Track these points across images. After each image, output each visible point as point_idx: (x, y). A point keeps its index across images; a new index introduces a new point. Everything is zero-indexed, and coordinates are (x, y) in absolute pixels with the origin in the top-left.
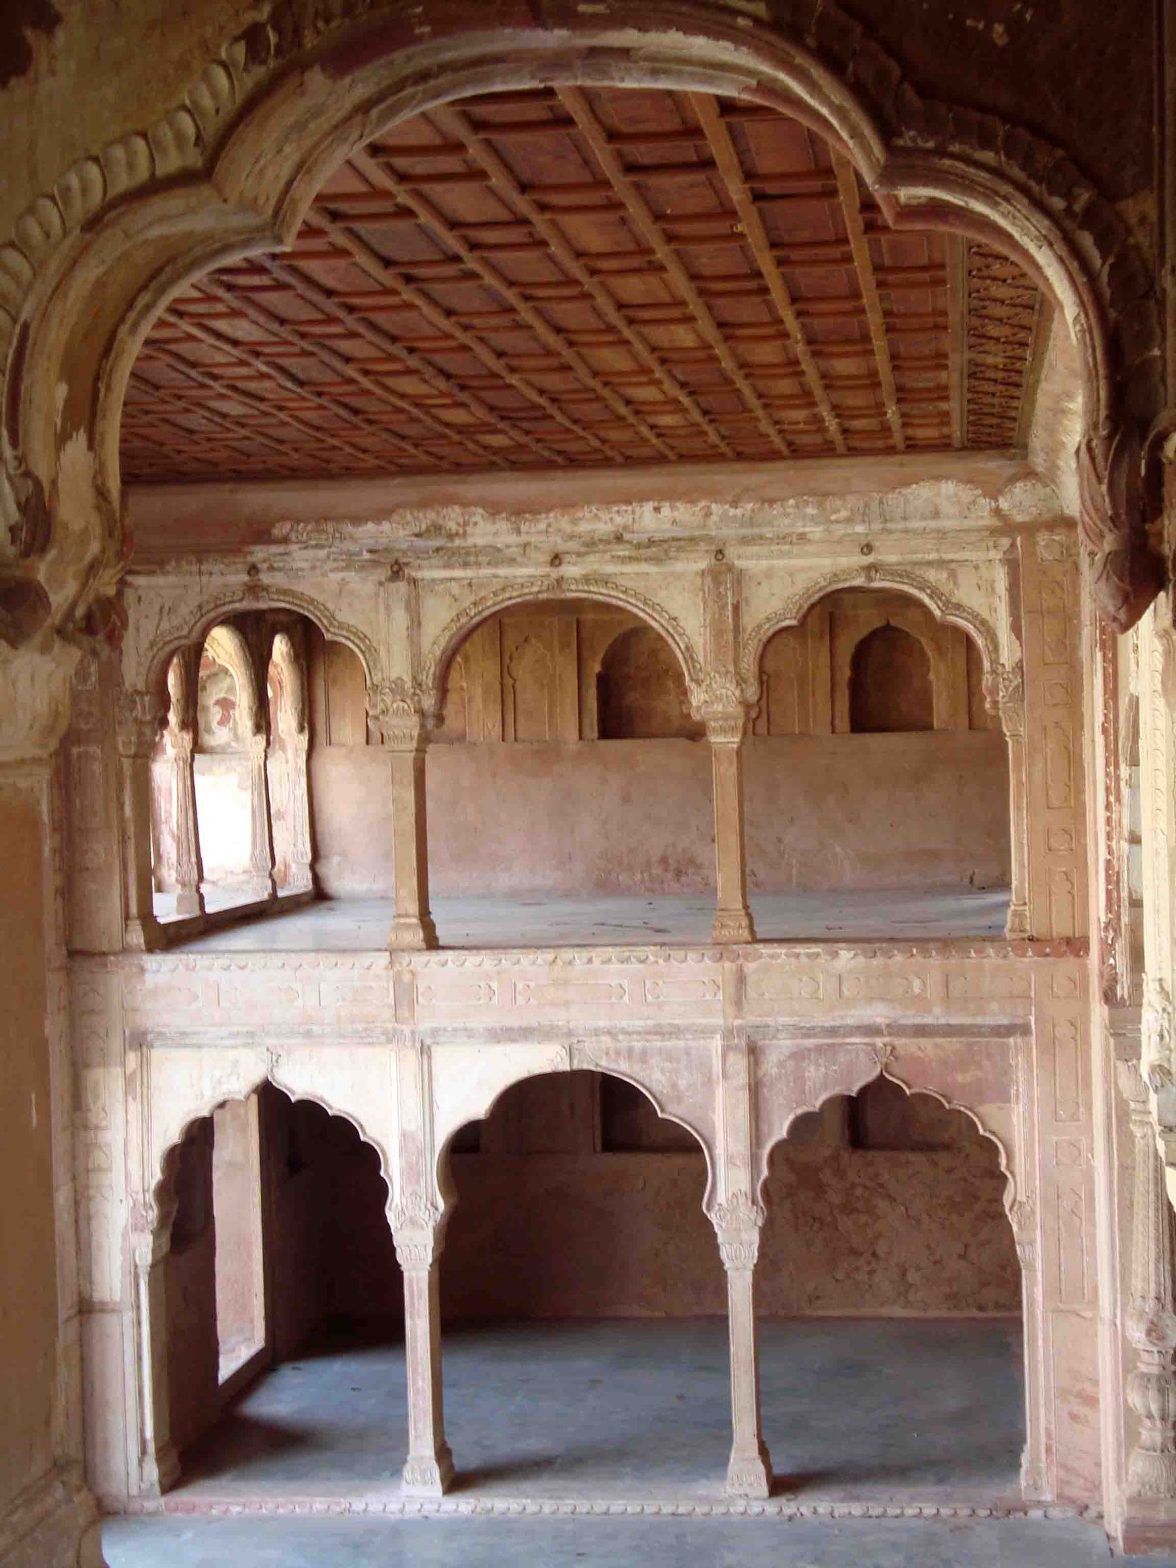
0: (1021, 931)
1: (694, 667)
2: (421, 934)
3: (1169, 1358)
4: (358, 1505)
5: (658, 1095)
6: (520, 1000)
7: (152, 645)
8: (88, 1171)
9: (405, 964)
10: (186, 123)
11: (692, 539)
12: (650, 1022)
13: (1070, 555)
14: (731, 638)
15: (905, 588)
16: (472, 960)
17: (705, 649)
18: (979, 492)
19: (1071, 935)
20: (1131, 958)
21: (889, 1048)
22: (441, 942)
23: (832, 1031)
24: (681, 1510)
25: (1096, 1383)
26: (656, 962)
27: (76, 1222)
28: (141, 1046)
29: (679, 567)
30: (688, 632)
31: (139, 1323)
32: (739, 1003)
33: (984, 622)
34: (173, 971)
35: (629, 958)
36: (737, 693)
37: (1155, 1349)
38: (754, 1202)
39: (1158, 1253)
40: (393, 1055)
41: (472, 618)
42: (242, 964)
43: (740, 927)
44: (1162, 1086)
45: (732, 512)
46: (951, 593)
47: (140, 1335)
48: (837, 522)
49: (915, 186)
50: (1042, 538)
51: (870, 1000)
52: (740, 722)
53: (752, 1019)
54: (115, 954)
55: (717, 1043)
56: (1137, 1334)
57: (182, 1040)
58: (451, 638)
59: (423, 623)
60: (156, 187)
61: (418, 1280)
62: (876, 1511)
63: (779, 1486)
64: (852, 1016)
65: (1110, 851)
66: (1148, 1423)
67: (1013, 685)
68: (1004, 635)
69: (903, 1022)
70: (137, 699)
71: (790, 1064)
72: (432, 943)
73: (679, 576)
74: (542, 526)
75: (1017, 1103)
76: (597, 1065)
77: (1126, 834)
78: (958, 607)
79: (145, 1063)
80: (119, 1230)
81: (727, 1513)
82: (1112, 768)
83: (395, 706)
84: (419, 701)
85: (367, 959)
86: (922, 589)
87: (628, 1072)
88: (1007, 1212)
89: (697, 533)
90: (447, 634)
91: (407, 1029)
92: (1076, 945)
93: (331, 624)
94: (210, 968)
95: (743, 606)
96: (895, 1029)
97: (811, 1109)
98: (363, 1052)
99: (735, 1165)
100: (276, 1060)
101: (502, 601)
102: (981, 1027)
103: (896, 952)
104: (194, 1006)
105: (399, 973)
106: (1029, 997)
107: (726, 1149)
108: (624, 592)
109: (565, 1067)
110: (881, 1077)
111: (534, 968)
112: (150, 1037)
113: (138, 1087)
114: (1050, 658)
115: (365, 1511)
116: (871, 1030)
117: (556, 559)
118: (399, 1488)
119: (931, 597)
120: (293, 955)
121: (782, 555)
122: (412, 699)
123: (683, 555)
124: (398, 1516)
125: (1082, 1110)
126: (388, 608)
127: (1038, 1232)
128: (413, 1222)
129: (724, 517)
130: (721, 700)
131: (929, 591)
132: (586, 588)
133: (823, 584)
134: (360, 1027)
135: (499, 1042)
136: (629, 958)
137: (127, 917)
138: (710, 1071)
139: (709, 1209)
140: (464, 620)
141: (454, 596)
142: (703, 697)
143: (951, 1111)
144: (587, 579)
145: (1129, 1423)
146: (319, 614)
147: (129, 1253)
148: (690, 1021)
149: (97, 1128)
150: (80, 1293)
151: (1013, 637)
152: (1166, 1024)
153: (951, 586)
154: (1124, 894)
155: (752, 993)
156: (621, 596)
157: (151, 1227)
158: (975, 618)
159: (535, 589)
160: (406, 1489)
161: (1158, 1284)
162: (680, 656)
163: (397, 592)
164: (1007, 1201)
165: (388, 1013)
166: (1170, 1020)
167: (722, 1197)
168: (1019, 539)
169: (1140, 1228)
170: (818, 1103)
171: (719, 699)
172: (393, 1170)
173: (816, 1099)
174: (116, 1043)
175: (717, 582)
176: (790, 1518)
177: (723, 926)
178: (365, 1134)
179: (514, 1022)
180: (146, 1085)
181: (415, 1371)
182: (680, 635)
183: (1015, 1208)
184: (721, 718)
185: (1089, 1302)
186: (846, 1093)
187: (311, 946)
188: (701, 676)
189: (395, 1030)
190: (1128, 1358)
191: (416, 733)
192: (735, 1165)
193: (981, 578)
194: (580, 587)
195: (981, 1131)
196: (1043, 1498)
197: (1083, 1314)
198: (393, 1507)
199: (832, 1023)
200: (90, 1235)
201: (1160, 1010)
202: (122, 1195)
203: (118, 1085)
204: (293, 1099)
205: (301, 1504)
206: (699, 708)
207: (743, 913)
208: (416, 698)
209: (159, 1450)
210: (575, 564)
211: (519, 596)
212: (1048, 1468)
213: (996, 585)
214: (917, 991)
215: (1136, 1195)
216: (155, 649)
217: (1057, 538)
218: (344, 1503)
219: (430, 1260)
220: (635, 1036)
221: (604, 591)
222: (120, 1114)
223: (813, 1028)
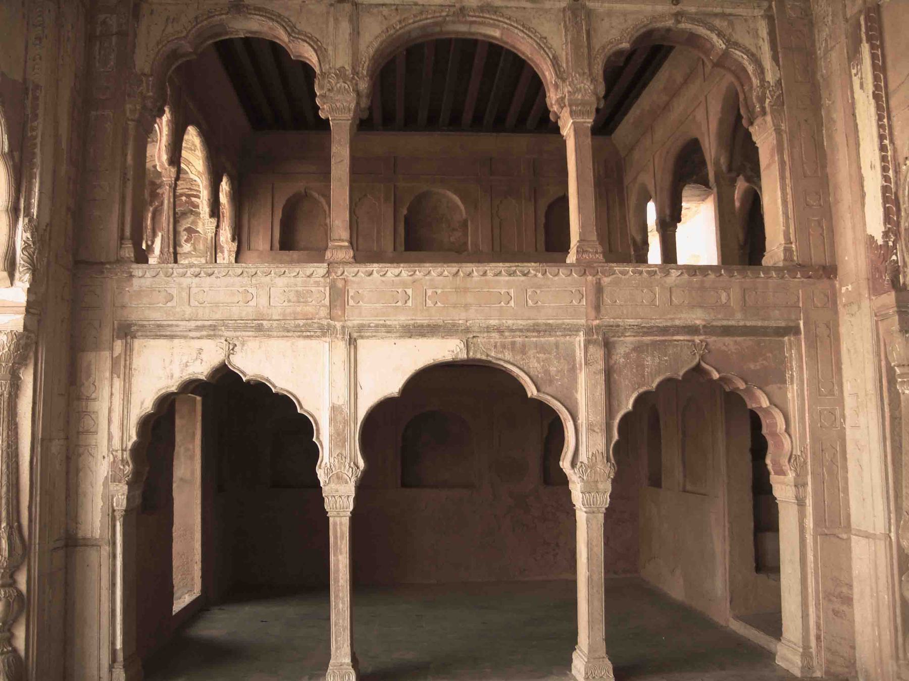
0: (791, 261)
1: (560, 71)
2: (351, 253)
5: (535, 378)
6: (429, 303)
7: (158, 44)
8: (78, 433)
9: (339, 273)
12: (531, 322)
13: (807, 15)
14: (586, 50)
17: (567, 58)
19: (824, 264)
21: (704, 344)
23: (664, 331)
25: (850, 586)
26: (536, 275)
27: (67, 473)
28: (126, 335)
30: (555, 46)
31: (114, 556)
32: (597, 308)
33: (753, 55)
35: (515, 272)
36: (592, 87)
38: (608, 460)
40: (327, 345)
41: (397, 31)
42: (210, 271)
43: (596, 252)
46: (730, 34)
47: (114, 565)
49: (455, 194)
51: (692, 307)
53: (608, 320)
54: (109, 263)
55: (581, 338)
57: (160, 332)
58: (382, 43)
59: (361, 32)
61: (341, 523)
64: (680, 319)
67: (777, 93)
68: (768, 63)
69: (715, 323)
70: (144, 79)
71: (634, 355)
73: (546, 11)
75: (792, 383)
76: (488, 355)
79: (128, 350)
82: (885, 120)
83: (338, 85)
84: (357, 84)
90: (379, 40)
91: (338, 325)
93: (293, 30)
94: (184, 275)
95: (592, 33)
96: (709, 330)
97: (650, 388)
98: (302, 343)
99: (594, 431)
100: (232, 350)
101: (421, 20)
102: (767, 327)
103: (710, 272)
104: (169, 304)
105: (334, 281)
106: (799, 307)
107: (587, 418)
108: (509, 19)
109: (463, 356)
110: (699, 365)
111: (441, 278)
112: (134, 328)
113: (122, 367)
114: (800, 78)
116: (692, 330)
119: (719, 35)
122: (351, 82)
125: (836, 387)
126: (336, 20)
127: (809, 477)
128: (339, 478)
130: (580, 91)
131: (717, 32)
132: (481, 15)
134: (301, 322)
136: (515, 272)
137: (122, 238)
138: (574, 360)
140: (392, 31)
141: (384, 16)
146: (284, 24)
147: (108, 498)
148: (560, 322)
150: (67, 531)
151: (774, 64)
153: (731, 31)
155: (607, 300)
156: (508, 21)
158: (747, 51)
159: (444, 14)
163: (344, 10)
165: (324, 312)
170: (654, 385)
171: (579, 90)
172: (324, 436)
173: (653, 382)
174: (107, 333)
175: (575, 14)
178: (301, 407)
179: (422, 320)
180: (129, 368)
181: (337, 596)
182: (549, 49)
183: (792, 461)
184: (580, 104)
185: (845, 527)
186: (675, 376)
188: (565, 76)
189: (329, 324)
191: (353, 106)
192: (594, 431)
193: (749, 27)
194: (477, 14)
196: (814, 675)
197: (840, 536)
199: (665, 324)
200: (77, 486)
202: (105, 452)
204: (244, 379)
208: (354, 82)
209: (125, 659)
211: (433, 17)
212: (818, 652)
213: (760, 32)
214: (724, 300)
216: (160, 47)
217: (798, 4)
219: (351, 508)
220: (518, 333)
221: (495, 17)
223: (652, 327)
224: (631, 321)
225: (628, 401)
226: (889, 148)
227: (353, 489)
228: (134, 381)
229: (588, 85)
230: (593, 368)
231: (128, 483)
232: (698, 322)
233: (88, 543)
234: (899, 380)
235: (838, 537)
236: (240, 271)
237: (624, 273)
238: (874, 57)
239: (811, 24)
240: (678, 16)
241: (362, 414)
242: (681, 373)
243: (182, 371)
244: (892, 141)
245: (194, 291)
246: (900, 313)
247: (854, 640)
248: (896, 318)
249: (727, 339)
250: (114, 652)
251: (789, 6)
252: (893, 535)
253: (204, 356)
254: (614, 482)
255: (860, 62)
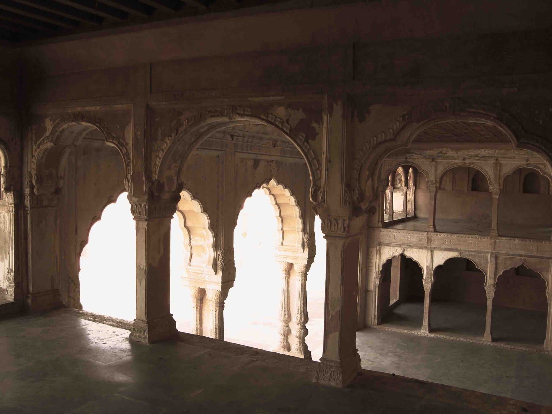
2: (433, 229)
4: (413, 332)
8: (368, 267)
10: (391, 131)
11: (492, 157)
15: (535, 169)
16: (442, 235)
22: (437, 231)
23: (513, 255)
24: (474, 342)
28: (380, 245)
29: (488, 162)
31: (376, 295)
32: (494, 248)
34: (386, 232)
36: (499, 187)
38: (494, 286)
41: (447, 169)
45: (500, 152)
48: (521, 155)
52: (499, 193)
54: (376, 228)
55: (489, 255)
57: (387, 245)
58: (444, 172)
60: (385, 141)
62: (513, 347)
63: (494, 340)
72: (435, 231)
74: (462, 153)
76: (465, 257)
78: (546, 173)
79: (380, 248)
80: (373, 278)
81: (483, 344)
83: (431, 185)
84: (436, 185)
85: (423, 233)
86: (539, 169)
87: (471, 259)
88: (546, 293)
89: (493, 155)
90: (442, 172)
94: (393, 232)
96: (526, 256)
100: (404, 251)
108: (478, 166)
109: (459, 257)
110: (522, 265)
115: (414, 333)
116: (521, 256)
117: (464, 159)
118: (420, 330)
119: (540, 171)
120: (409, 231)
121: (509, 161)
123: (490, 160)
124: (420, 335)
128: (427, 283)
129: (498, 153)
133: (518, 167)
134: (420, 245)
135: (446, 251)
137: (379, 221)
138: (488, 260)
139: (485, 286)
142: (492, 187)
143: (536, 273)
144: (470, 163)
149: (371, 259)
156: (477, 167)
157: (379, 278)
159: (460, 165)
160: (422, 331)
162: (488, 179)
164: (547, 291)
165: (426, 243)
167: (488, 284)
170: (509, 269)
174: (375, 244)
176: (496, 346)
177: (493, 233)
181: (425, 310)
182: (488, 175)
187: (413, 229)
189: (427, 247)
195: (542, 277)
198: (419, 333)
203: (375, 251)
204: (407, 257)
205: (402, 331)
206: (491, 190)
207: (496, 230)
210: (468, 160)
218: (410, 332)
219: (430, 290)
222: (375, 257)
223: (509, 254)
224: (504, 252)
225: (501, 272)
227: (431, 286)
228: (381, 255)
229: (498, 187)
230: (492, 263)
231: (379, 279)
232: (523, 254)
233: (370, 291)
236: (406, 232)
237: (502, 239)
240: (527, 164)
241: (434, 268)
242: (517, 266)
243: (393, 254)
245: (396, 236)
249: (531, 259)
250: (375, 316)
253: (398, 251)
254: (495, 292)
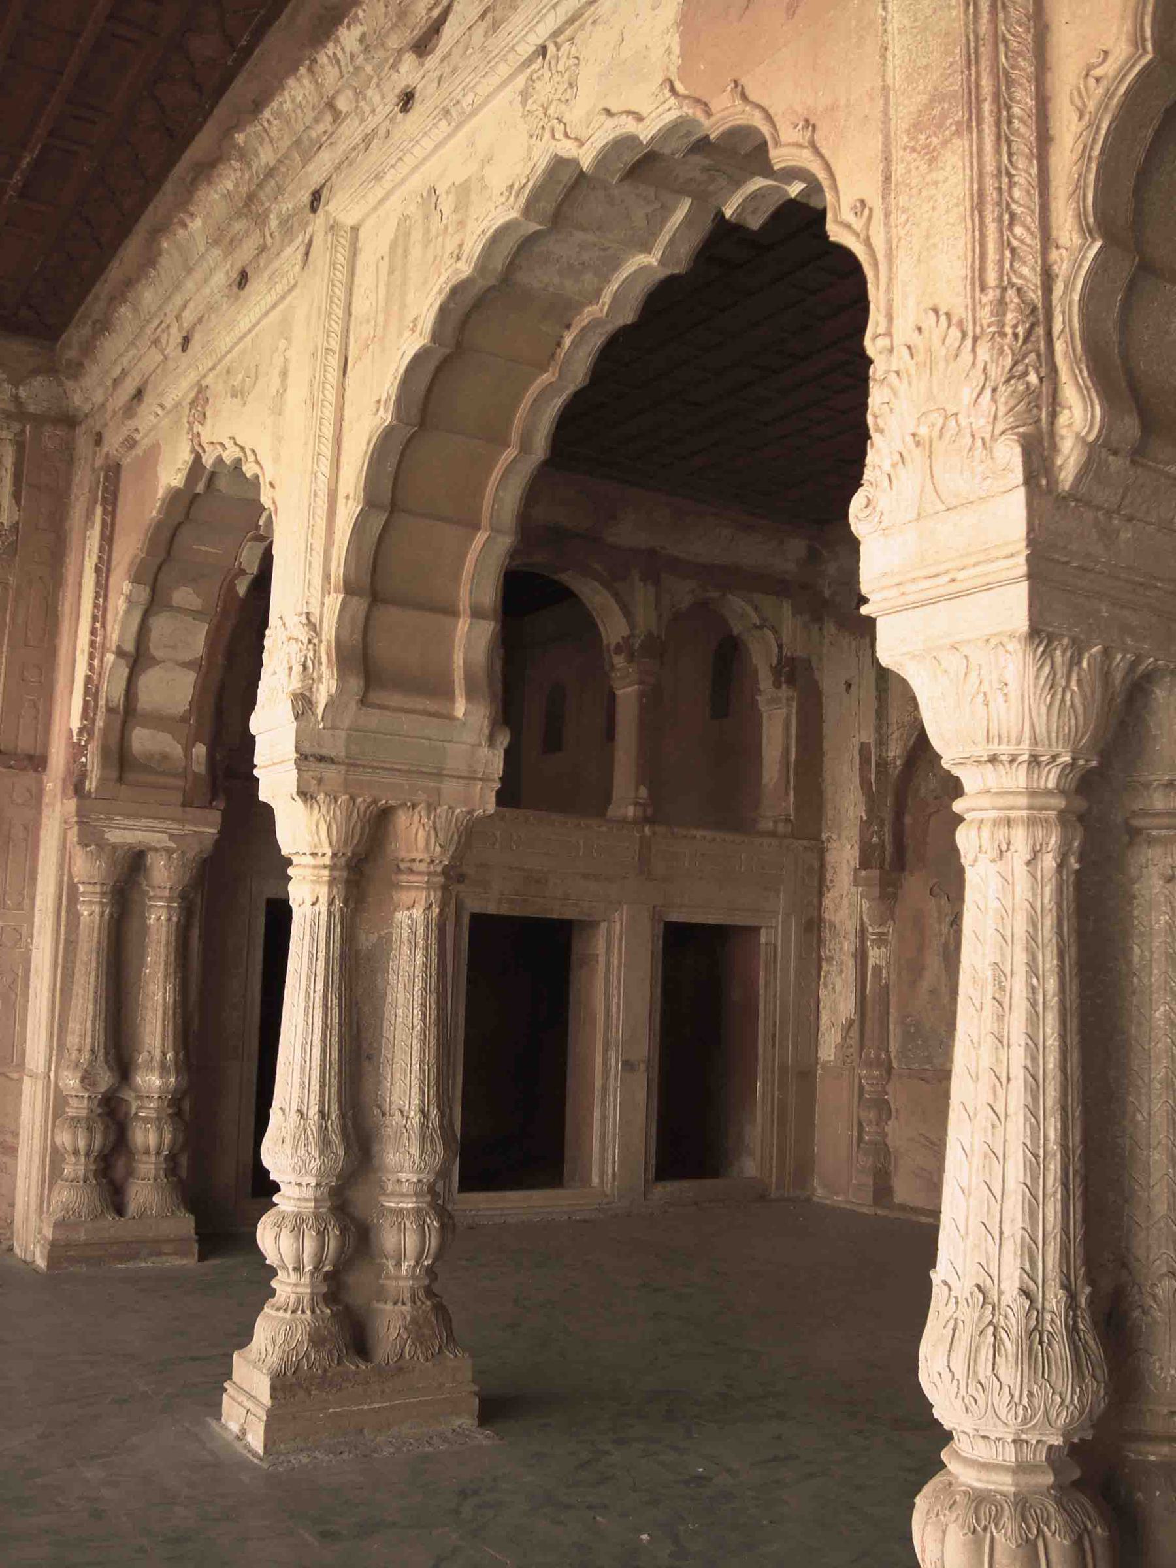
3: (96, 1102)
13: (67, 448)
18: (4, 376)
19: (32, 753)
20: (102, 758)
25: (16, 1135)
37: (86, 1095)
39: (95, 1012)
44: (303, 713)
50: (48, 430)
56: (71, 1082)
65: (91, 667)
66: (73, 1159)
67: (11, 539)
77: (114, 648)
82: (101, 600)
92: (38, 762)
125: (26, 901)
145: (55, 1157)
152: (311, 654)
154: (102, 702)
161: (93, 1037)
166: (315, 651)
168: (28, 427)
169: (81, 992)
185: (17, 1065)
190: (58, 1103)
201: (306, 641)
215: (78, 963)
226: (99, 632)
234: (82, 899)
235: (7, 1077)
238: (104, 522)
239: (71, 462)
244: (104, 626)
246: (80, 823)
247: (14, 1198)
248: (76, 829)
251: (47, 434)
252: (52, 1075)
255: (93, 527)
